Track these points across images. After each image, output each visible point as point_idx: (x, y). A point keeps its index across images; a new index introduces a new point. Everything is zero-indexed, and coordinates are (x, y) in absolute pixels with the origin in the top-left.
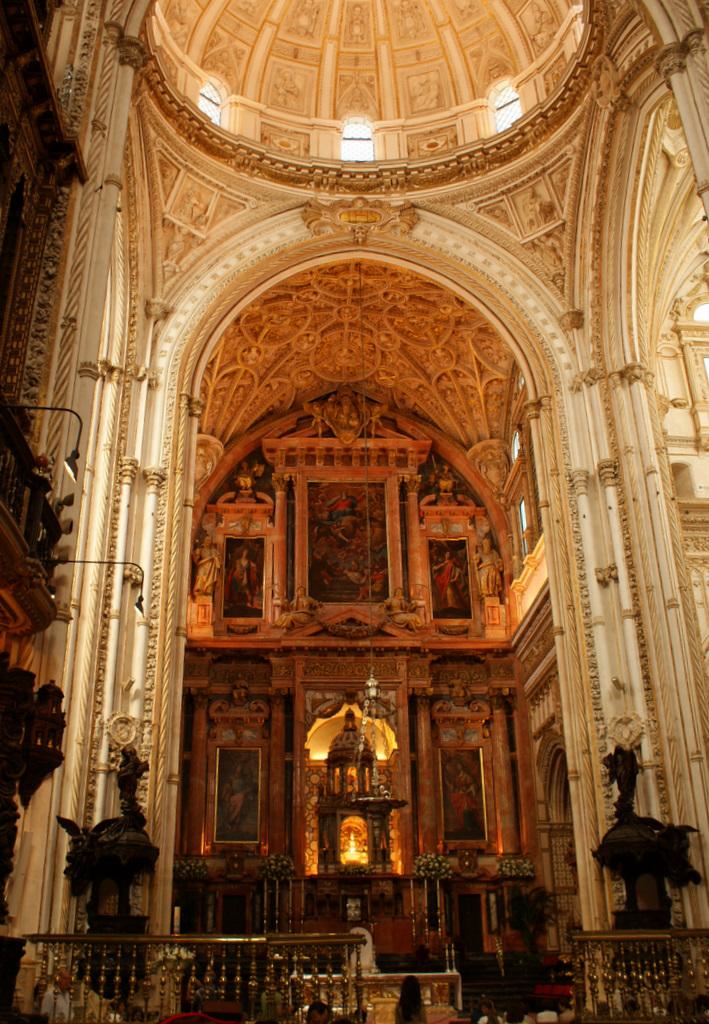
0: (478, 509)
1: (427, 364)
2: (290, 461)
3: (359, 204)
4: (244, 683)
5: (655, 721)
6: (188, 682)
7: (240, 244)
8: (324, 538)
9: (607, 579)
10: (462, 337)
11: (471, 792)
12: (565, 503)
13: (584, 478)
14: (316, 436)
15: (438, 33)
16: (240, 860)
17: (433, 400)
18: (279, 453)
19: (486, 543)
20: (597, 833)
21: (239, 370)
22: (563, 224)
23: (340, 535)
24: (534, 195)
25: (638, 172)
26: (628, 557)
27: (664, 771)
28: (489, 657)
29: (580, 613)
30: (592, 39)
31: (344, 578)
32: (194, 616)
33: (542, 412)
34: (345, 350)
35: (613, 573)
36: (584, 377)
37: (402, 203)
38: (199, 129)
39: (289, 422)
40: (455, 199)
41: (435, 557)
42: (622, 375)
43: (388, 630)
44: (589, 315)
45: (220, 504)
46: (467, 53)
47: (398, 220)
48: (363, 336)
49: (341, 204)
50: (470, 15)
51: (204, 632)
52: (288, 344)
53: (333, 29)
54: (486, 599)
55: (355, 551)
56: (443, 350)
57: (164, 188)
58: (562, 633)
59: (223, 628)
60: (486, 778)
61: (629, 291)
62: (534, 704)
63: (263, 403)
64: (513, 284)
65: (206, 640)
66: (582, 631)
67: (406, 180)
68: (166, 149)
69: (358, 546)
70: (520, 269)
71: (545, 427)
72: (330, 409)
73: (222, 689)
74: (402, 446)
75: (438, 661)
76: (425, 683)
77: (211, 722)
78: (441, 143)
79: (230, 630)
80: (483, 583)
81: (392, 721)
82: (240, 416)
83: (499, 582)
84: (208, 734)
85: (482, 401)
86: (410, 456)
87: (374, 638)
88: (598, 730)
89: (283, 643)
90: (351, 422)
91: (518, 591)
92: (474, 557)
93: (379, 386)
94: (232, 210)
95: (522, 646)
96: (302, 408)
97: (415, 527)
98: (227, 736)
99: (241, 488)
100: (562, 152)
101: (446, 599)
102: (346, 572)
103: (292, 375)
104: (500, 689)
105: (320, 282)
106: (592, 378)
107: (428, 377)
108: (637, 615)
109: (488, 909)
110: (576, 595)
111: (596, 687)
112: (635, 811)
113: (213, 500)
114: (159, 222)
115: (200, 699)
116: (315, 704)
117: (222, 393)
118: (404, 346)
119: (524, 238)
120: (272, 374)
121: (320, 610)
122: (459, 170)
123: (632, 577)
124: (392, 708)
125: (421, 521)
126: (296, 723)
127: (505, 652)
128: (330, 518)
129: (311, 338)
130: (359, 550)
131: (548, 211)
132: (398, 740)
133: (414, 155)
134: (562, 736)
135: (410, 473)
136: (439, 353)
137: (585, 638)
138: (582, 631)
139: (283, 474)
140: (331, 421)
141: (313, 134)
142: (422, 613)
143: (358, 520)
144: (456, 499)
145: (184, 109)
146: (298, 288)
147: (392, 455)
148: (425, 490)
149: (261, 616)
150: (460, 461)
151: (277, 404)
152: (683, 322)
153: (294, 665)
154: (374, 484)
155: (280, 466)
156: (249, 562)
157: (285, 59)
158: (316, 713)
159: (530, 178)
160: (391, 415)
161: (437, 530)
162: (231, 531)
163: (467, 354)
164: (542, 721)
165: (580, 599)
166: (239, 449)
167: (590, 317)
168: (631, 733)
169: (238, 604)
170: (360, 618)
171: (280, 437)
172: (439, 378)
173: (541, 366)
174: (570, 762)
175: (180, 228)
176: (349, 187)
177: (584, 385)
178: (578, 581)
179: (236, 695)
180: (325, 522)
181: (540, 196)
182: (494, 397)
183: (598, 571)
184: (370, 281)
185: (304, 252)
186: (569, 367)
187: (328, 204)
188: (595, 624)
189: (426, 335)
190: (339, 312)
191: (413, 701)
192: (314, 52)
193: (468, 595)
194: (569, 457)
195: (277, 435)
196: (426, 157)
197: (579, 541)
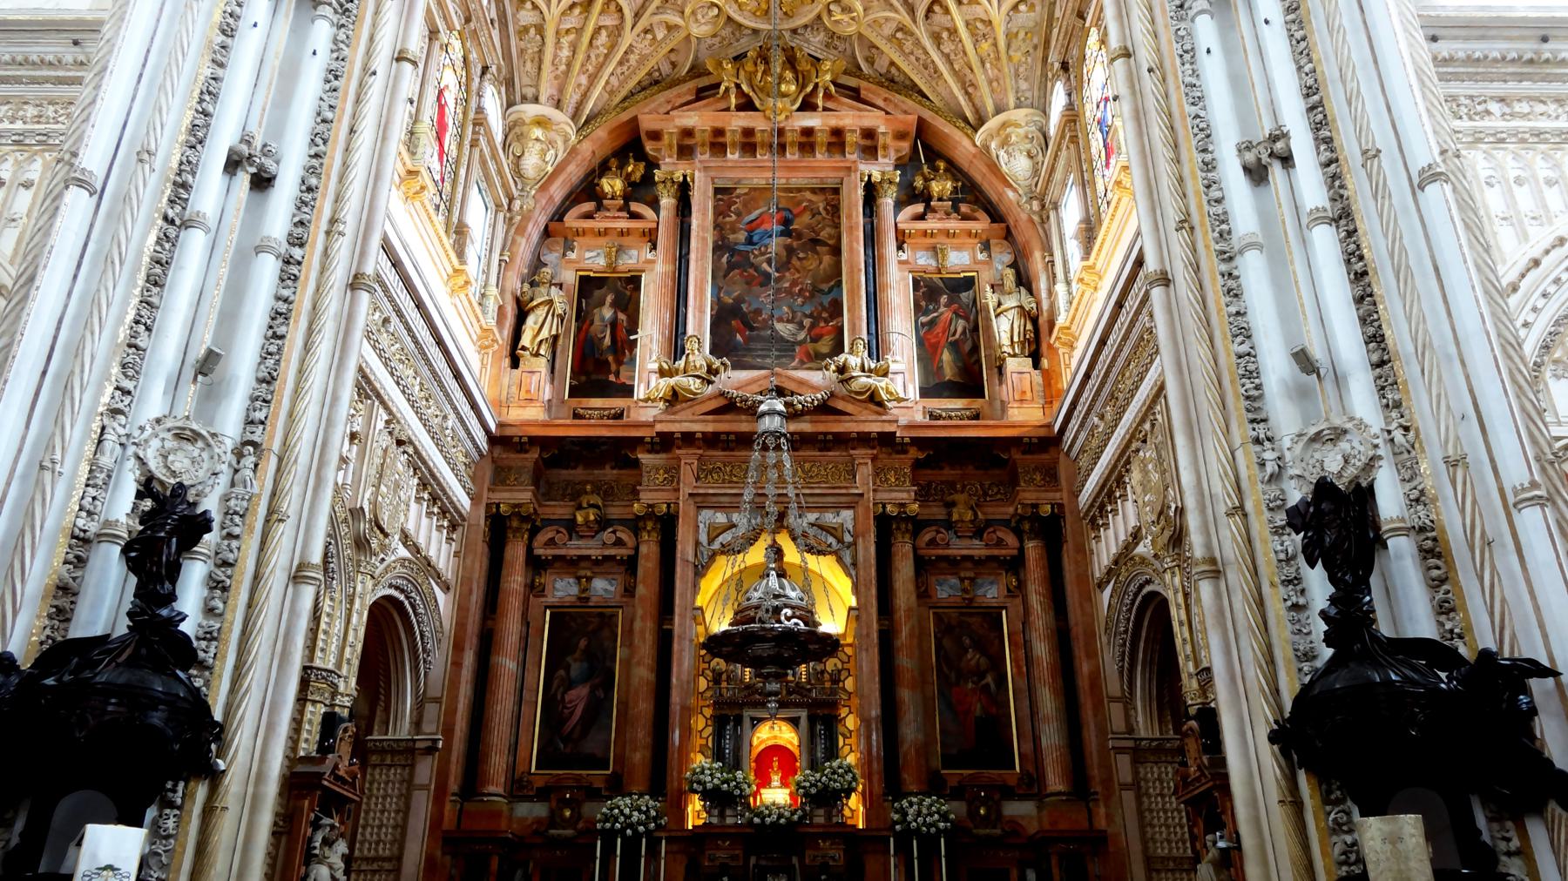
0: (995, 225)
2: (685, 152)
5: (1406, 429)
6: (497, 496)
8: (737, 271)
9: (1265, 158)
11: (988, 685)
12: (1166, 36)
14: (728, 109)
16: (575, 804)
19: (1010, 275)
20: (1276, 692)
26: (1311, 109)
28: (1017, 455)
32: (514, 389)
41: (923, 303)
43: (840, 405)
45: (571, 220)
54: (1009, 360)
55: (789, 292)
58: (1165, 280)
60: (1014, 660)
63: (643, 59)
69: (794, 283)
72: (749, 67)
73: (560, 510)
76: (905, 495)
80: (1005, 341)
81: (848, 560)
82: (602, 83)
83: (1030, 335)
86: (881, 140)
87: (815, 418)
88: (1262, 465)
89: (659, 428)
90: (783, 87)
91: (1064, 344)
92: (991, 299)
95: (1074, 424)
98: (563, 589)
99: (605, 196)
101: (940, 368)
103: (688, 11)
104: (1035, 506)
107: (911, 10)
108: (1343, 217)
115: (515, 524)
116: (715, 532)
117: (572, 37)
121: (723, 376)
124: (848, 538)
125: (900, 248)
126: (678, 561)
127: (1046, 443)
128: (750, 241)
132: (856, 589)
135: (880, 169)
138: (1211, 266)
139: (672, 173)
143: (795, 244)
147: (851, 138)
148: (909, 195)
149: (632, 396)
150: (963, 146)
151: (666, 69)
153: (679, 466)
154: (822, 190)
155: (667, 160)
156: (615, 313)
158: (716, 546)
160: (852, 82)
161: (924, 260)
162: (588, 264)
164: (1114, 550)
165: (1206, 207)
166: (600, 139)
169: (594, 377)
171: (668, 113)
172: (930, 10)
179: (580, 519)
180: (742, 248)
182: (1022, 35)
188: (1241, 252)
191: (886, 526)
193: (979, 362)
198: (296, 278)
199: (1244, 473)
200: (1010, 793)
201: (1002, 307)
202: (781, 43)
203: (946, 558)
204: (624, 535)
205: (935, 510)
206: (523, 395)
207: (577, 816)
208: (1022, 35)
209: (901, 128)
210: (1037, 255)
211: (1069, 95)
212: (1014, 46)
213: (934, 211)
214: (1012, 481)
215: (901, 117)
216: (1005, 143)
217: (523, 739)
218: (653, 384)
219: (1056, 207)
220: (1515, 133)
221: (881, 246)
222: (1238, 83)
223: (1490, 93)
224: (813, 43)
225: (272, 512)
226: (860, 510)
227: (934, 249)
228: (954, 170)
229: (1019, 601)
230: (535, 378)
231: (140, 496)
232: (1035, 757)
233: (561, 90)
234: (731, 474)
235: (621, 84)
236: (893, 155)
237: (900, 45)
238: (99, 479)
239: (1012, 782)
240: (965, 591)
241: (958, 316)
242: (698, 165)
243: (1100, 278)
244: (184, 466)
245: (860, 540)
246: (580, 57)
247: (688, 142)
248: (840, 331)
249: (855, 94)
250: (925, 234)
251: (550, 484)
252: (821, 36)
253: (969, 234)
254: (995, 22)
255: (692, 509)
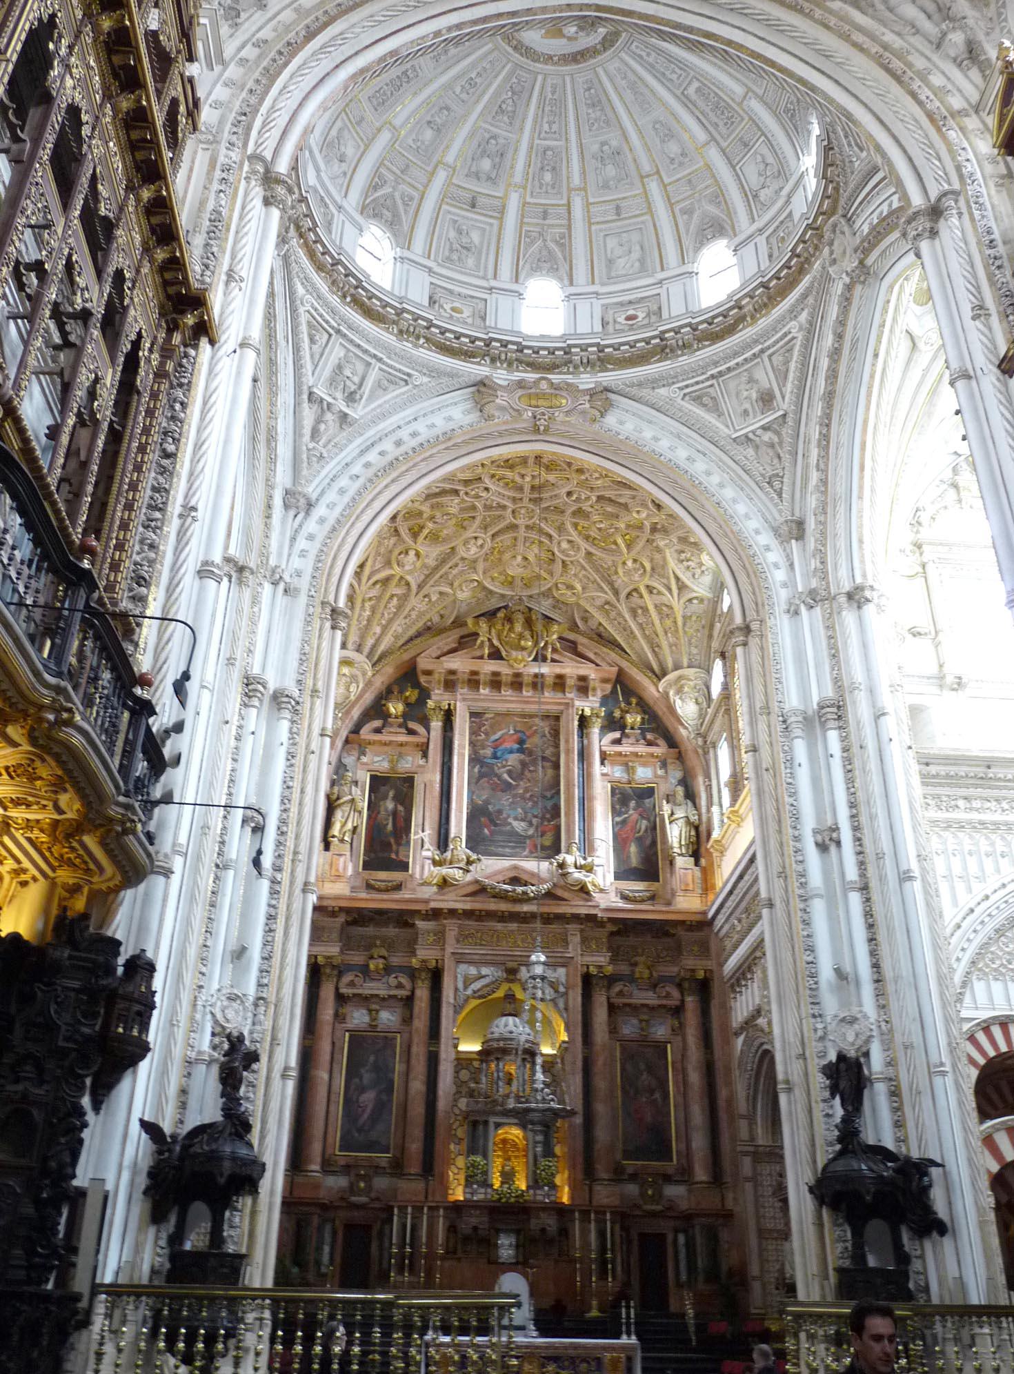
1: (614, 578)
3: (544, 385)
4: (384, 952)
6: (319, 950)
7: (399, 427)
9: (827, 842)
10: (657, 547)
12: (778, 748)
13: (800, 719)
14: (481, 657)
15: (643, 185)
16: (367, 1178)
17: (621, 620)
18: (436, 676)
19: (680, 791)
20: (815, 1162)
21: (393, 575)
22: (784, 416)
23: (506, 776)
24: (751, 380)
25: (876, 355)
26: (853, 816)
27: (898, 1087)
28: (681, 932)
29: (794, 884)
30: (825, 196)
31: (508, 828)
32: (327, 867)
33: (750, 638)
34: (519, 558)
35: (835, 835)
36: (803, 597)
37: (592, 386)
38: (356, 287)
39: (450, 640)
40: (654, 383)
42: (850, 596)
43: (559, 892)
44: (811, 524)
45: (366, 733)
46: (677, 209)
47: (587, 405)
48: (540, 542)
49: (521, 384)
50: (681, 164)
51: (339, 889)
52: (453, 548)
53: (518, 178)
55: (523, 797)
56: (635, 561)
57: (312, 356)
58: (771, 905)
59: (358, 883)
60: (675, 1083)
61: (860, 497)
62: (735, 992)
63: (421, 614)
64: (721, 485)
65: (337, 898)
66: (797, 904)
67: (599, 359)
68: (316, 310)
69: (526, 790)
70: (729, 467)
71: (755, 657)
72: (499, 627)
73: (357, 958)
74: (582, 672)
75: (618, 933)
76: (602, 959)
77: (341, 999)
78: (641, 315)
79: (369, 887)
80: (676, 844)
81: (561, 1005)
83: (693, 839)
84: (336, 1015)
85: (680, 623)
86: (592, 684)
88: (816, 1030)
89: (433, 905)
90: (523, 643)
92: (666, 809)
93: (558, 601)
94: (392, 387)
96: (465, 624)
97: (597, 768)
98: (358, 1018)
99: (389, 715)
100: (785, 330)
101: (628, 857)
102: (510, 820)
103: (456, 584)
104: (693, 971)
105: (493, 476)
106: (814, 598)
107: (616, 593)
108: (865, 888)
109: (676, 1253)
110: (791, 861)
111: (813, 976)
112: (862, 1135)
113: (356, 730)
114: (305, 397)
115: (328, 971)
118: (589, 554)
119: (736, 431)
120: (431, 582)
122: (662, 349)
123: (858, 840)
124: (562, 989)
125: (602, 763)
127: (702, 925)
128: (495, 757)
129: (480, 542)
130: (528, 795)
131: (767, 399)
132: (567, 1029)
133: (610, 328)
134: (771, 1033)
135: (589, 705)
136: (630, 563)
137: (800, 914)
140: (500, 640)
141: (491, 299)
142: (599, 870)
143: (527, 759)
144: (645, 739)
145: (339, 262)
146: (466, 482)
147: (570, 682)
150: (651, 690)
151: (436, 619)
152: (925, 534)
157: (461, 208)
158: (469, 992)
159: (746, 360)
162: (376, 766)
163: (665, 565)
166: (389, 671)
167: (813, 526)
168: (857, 1035)
169: (381, 855)
170: (525, 877)
171: (438, 658)
172: (629, 594)
173: (751, 584)
174: (780, 1068)
175: (329, 405)
176: (530, 364)
177: (803, 608)
178: (792, 843)
179: (372, 967)
181: (757, 382)
182: (694, 618)
183: (816, 832)
184: (551, 478)
185: (476, 440)
186: (785, 585)
187: (505, 383)
189: (615, 543)
190: (513, 512)
191: (587, 980)
192: (497, 203)
193: (656, 854)
194: (783, 694)
195: (434, 655)
196: (623, 331)
197: (793, 794)
198: (278, 892)
199: (806, 1034)
200: (668, 1179)
201: (675, 816)
202: (521, 608)
203: (629, 1005)
204: (404, 980)
205: (623, 967)
206: (334, 873)
207: (369, 1187)
208: (694, 618)
209: (606, 675)
210: (700, 779)
211: (725, 676)
212: (688, 624)
213: (628, 736)
214: (678, 949)
215: (608, 668)
216: (679, 691)
217: (330, 1129)
218: (426, 868)
219: (714, 746)
220: (970, 822)
221: (590, 765)
222: (816, 781)
223: (959, 794)
224: (545, 607)
225: (274, 1038)
226: (571, 968)
227: (626, 765)
228: (644, 707)
229: (679, 1038)
230: (342, 859)
231: (213, 1034)
232: (688, 1154)
233: (363, 637)
234: (481, 939)
235: (404, 632)
236: (599, 693)
237: (607, 612)
238: (194, 1027)
239: (670, 1171)
240: (642, 1029)
241: (643, 818)
242: (459, 697)
243: (742, 820)
244: (239, 1022)
245: (571, 993)
246: (378, 616)
247: (452, 677)
248: (558, 828)
249: (573, 648)
250: (620, 754)
251: (349, 938)
252: (550, 601)
253: (652, 755)
254: (676, 609)
255: (453, 964)
